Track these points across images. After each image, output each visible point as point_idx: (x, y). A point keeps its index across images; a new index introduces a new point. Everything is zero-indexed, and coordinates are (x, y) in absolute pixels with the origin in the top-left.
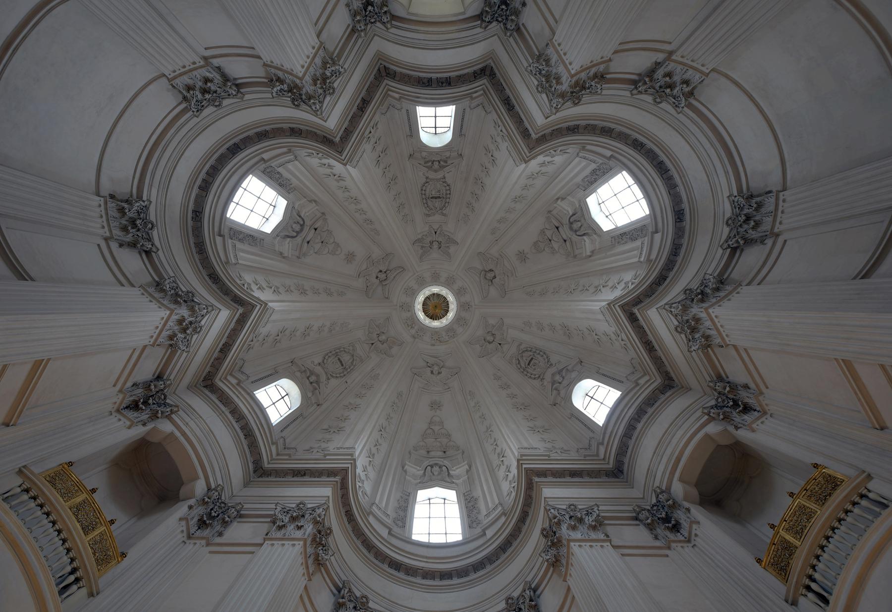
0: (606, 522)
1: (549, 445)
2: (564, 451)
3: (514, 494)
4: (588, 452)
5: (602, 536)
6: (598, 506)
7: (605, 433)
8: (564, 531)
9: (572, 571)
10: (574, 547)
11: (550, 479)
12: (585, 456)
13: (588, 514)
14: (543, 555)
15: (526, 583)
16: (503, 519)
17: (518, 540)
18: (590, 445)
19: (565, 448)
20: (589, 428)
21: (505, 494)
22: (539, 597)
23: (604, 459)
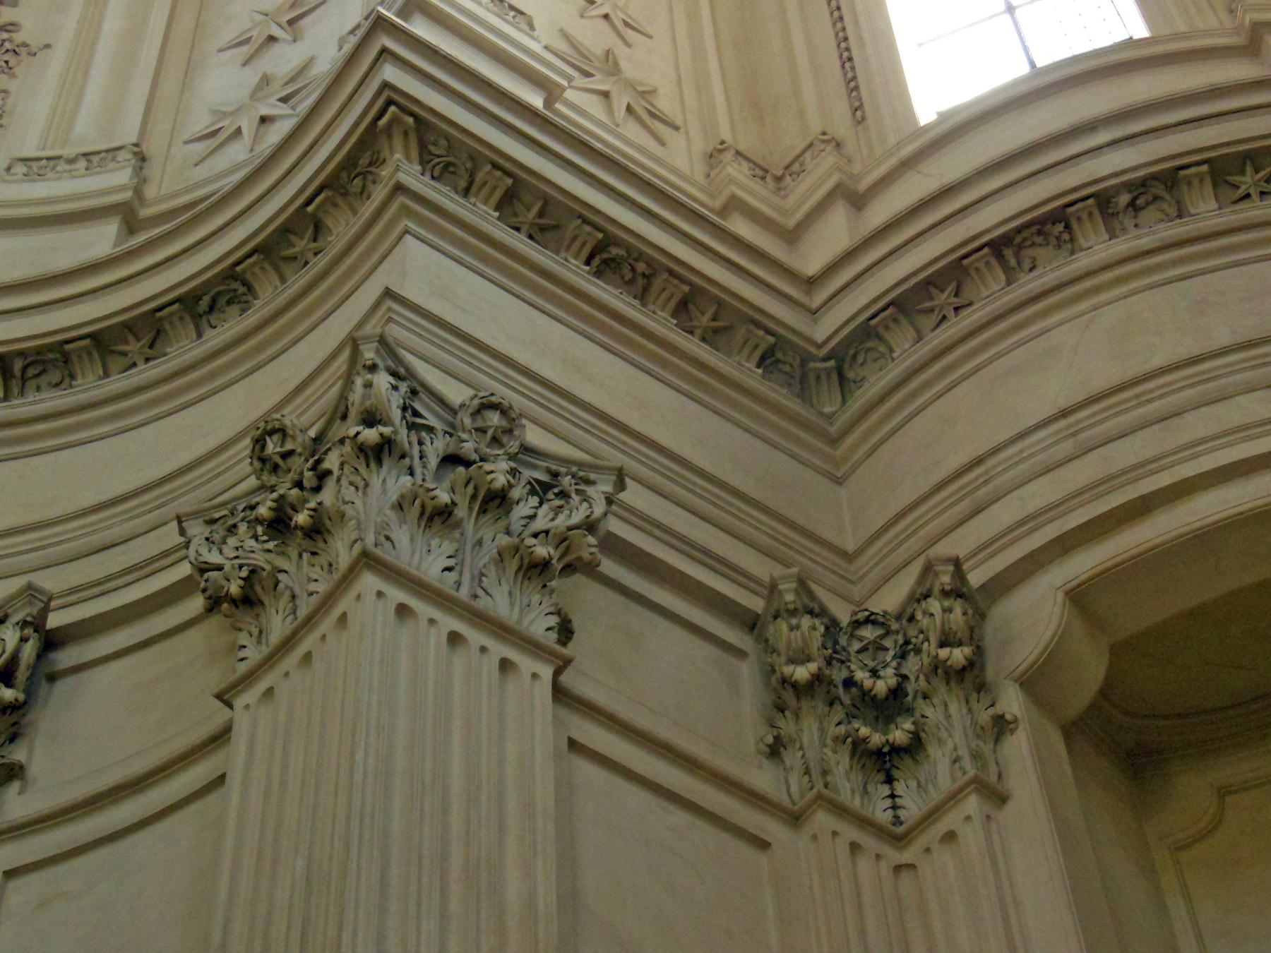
0: (608, 567)
1: (595, 37)
2: (646, 112)
3: (238, 153)
4: (757, 195)
5: (540, 625)
6: (621, 480)
7: (908, 164)
8: (369, 502)
9: (287, 679)
10: (371, 597)
11: (481, 214)
12: (733, 205)
13: (541, 490)
14: (197, 530)
15: (31, 591)
16: (101, 239)
17: (118, 383)
18: (794, 167)
19: (665, 104)
20: (852, 86)
21: (199, 122)
22: (52, 678)
23: (811, 283)
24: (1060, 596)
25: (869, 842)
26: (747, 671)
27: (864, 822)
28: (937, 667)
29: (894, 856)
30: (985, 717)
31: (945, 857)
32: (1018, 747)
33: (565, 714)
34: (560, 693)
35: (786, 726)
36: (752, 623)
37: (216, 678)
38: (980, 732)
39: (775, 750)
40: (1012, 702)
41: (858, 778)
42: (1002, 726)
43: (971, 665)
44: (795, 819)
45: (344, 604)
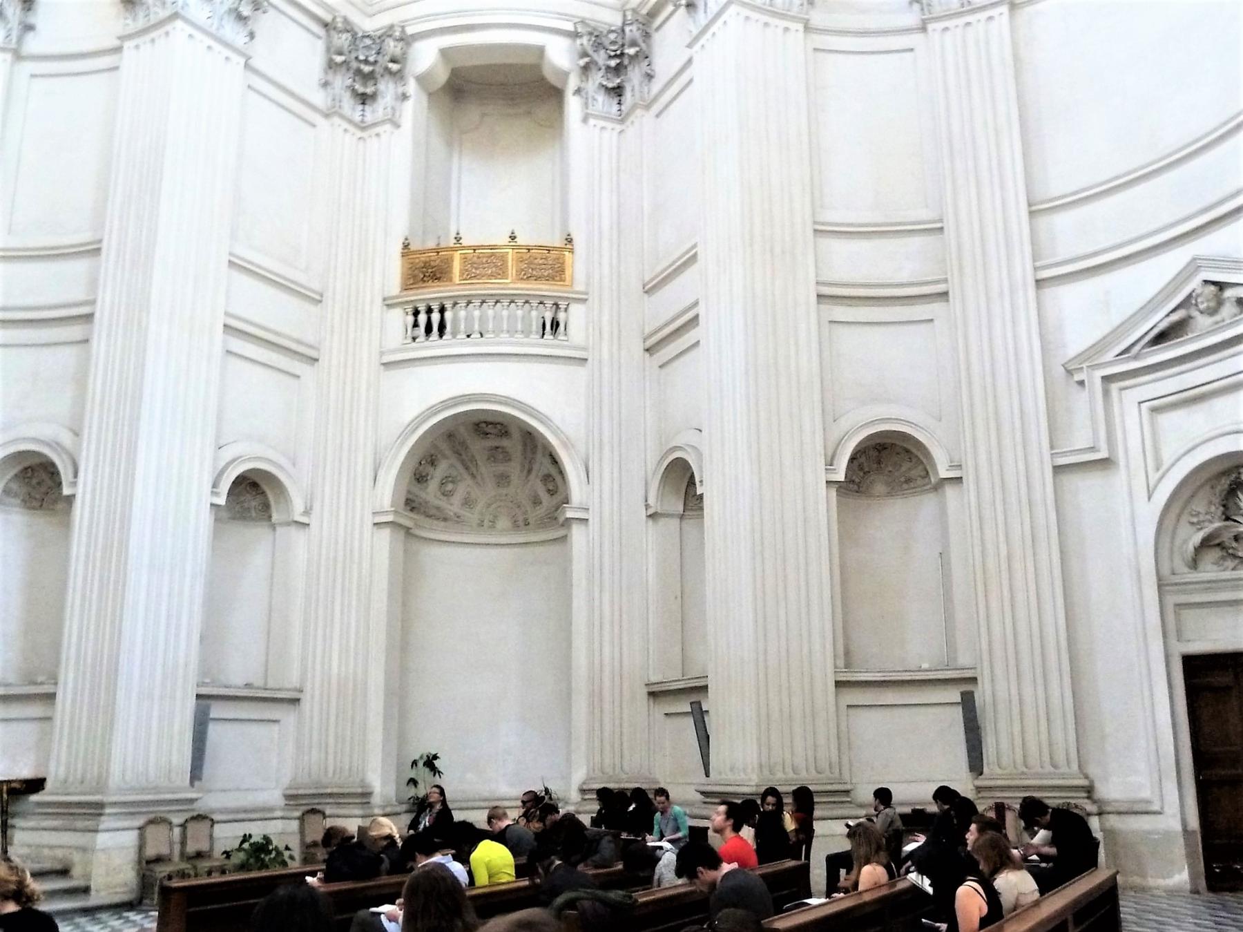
24: (436, 51)
25: (351, 129)
26: (320, 45)
27: (350, 121)
28: (387, 69)
29: (359, 134)
30: (400, 90)
31: (375, 139)
32: (409, 106)
33: (249, 74)
34: (247, 65)
35: (330, 77)
36: (326, 25)
37: (121, 32)
38: (397, 99)
39: (325, 85)
40: (412, 87)
41: (352, 102)
42: (405, 97)
43: (399, 71)
44: (327, 116)
45: (168, 27)
